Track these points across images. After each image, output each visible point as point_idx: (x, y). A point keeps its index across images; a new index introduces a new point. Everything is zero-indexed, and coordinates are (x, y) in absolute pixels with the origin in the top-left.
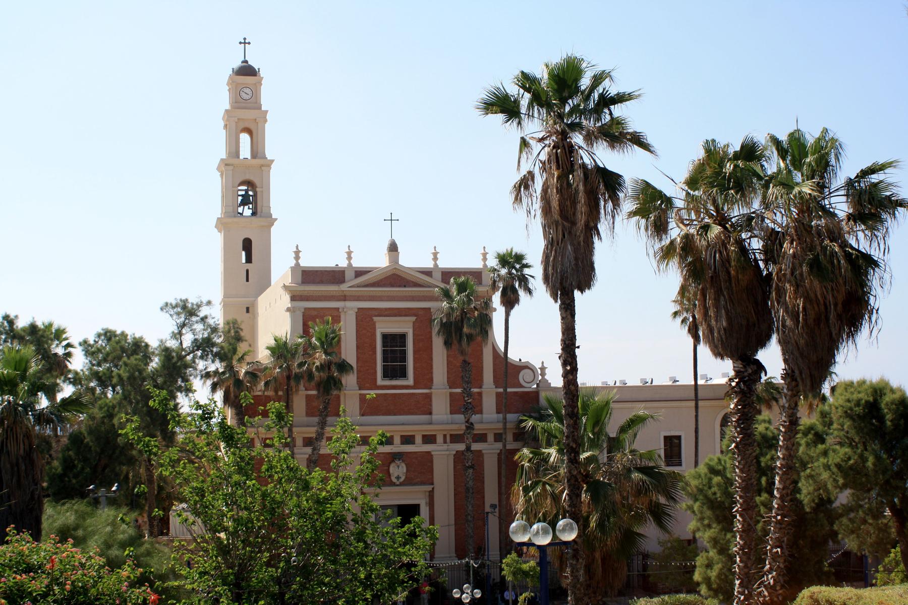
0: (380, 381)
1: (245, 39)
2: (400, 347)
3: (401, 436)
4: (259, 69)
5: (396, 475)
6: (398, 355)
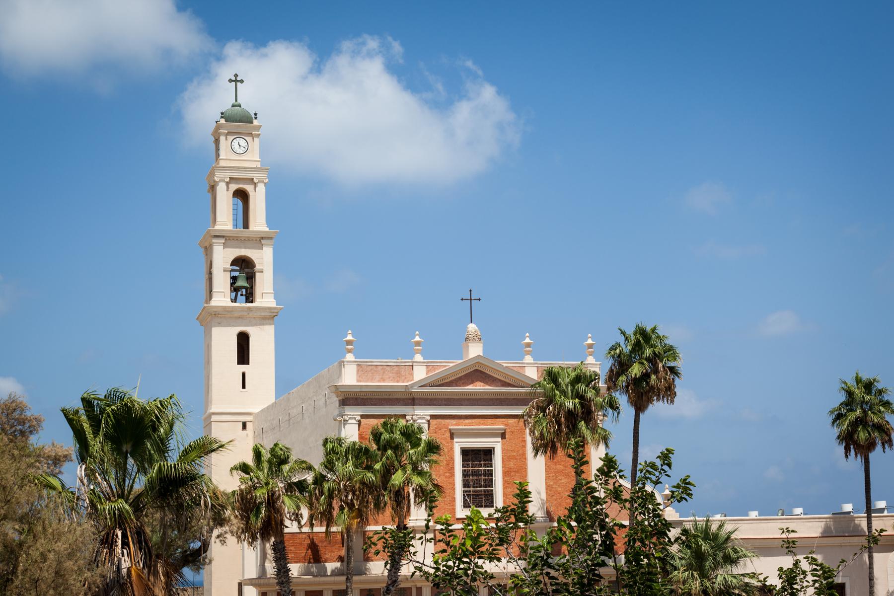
1: (236, 75)
2: (485, 465)
4: (256, 114)
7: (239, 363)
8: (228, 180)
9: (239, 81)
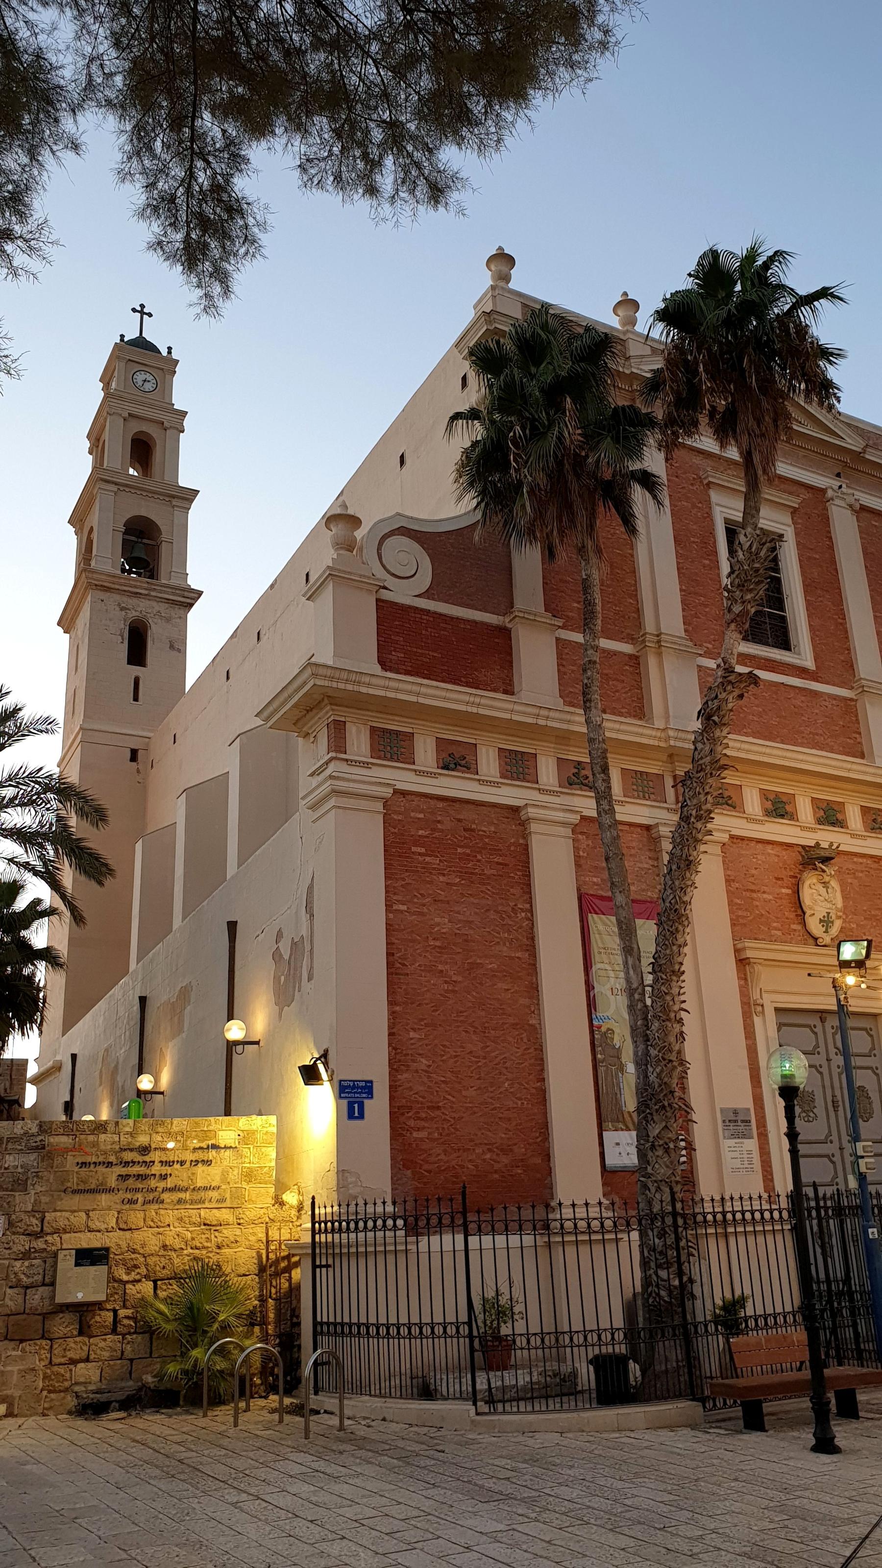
5: (821, 912)
7: (130, 662)
8: (126, 415)
9: (146, 314)
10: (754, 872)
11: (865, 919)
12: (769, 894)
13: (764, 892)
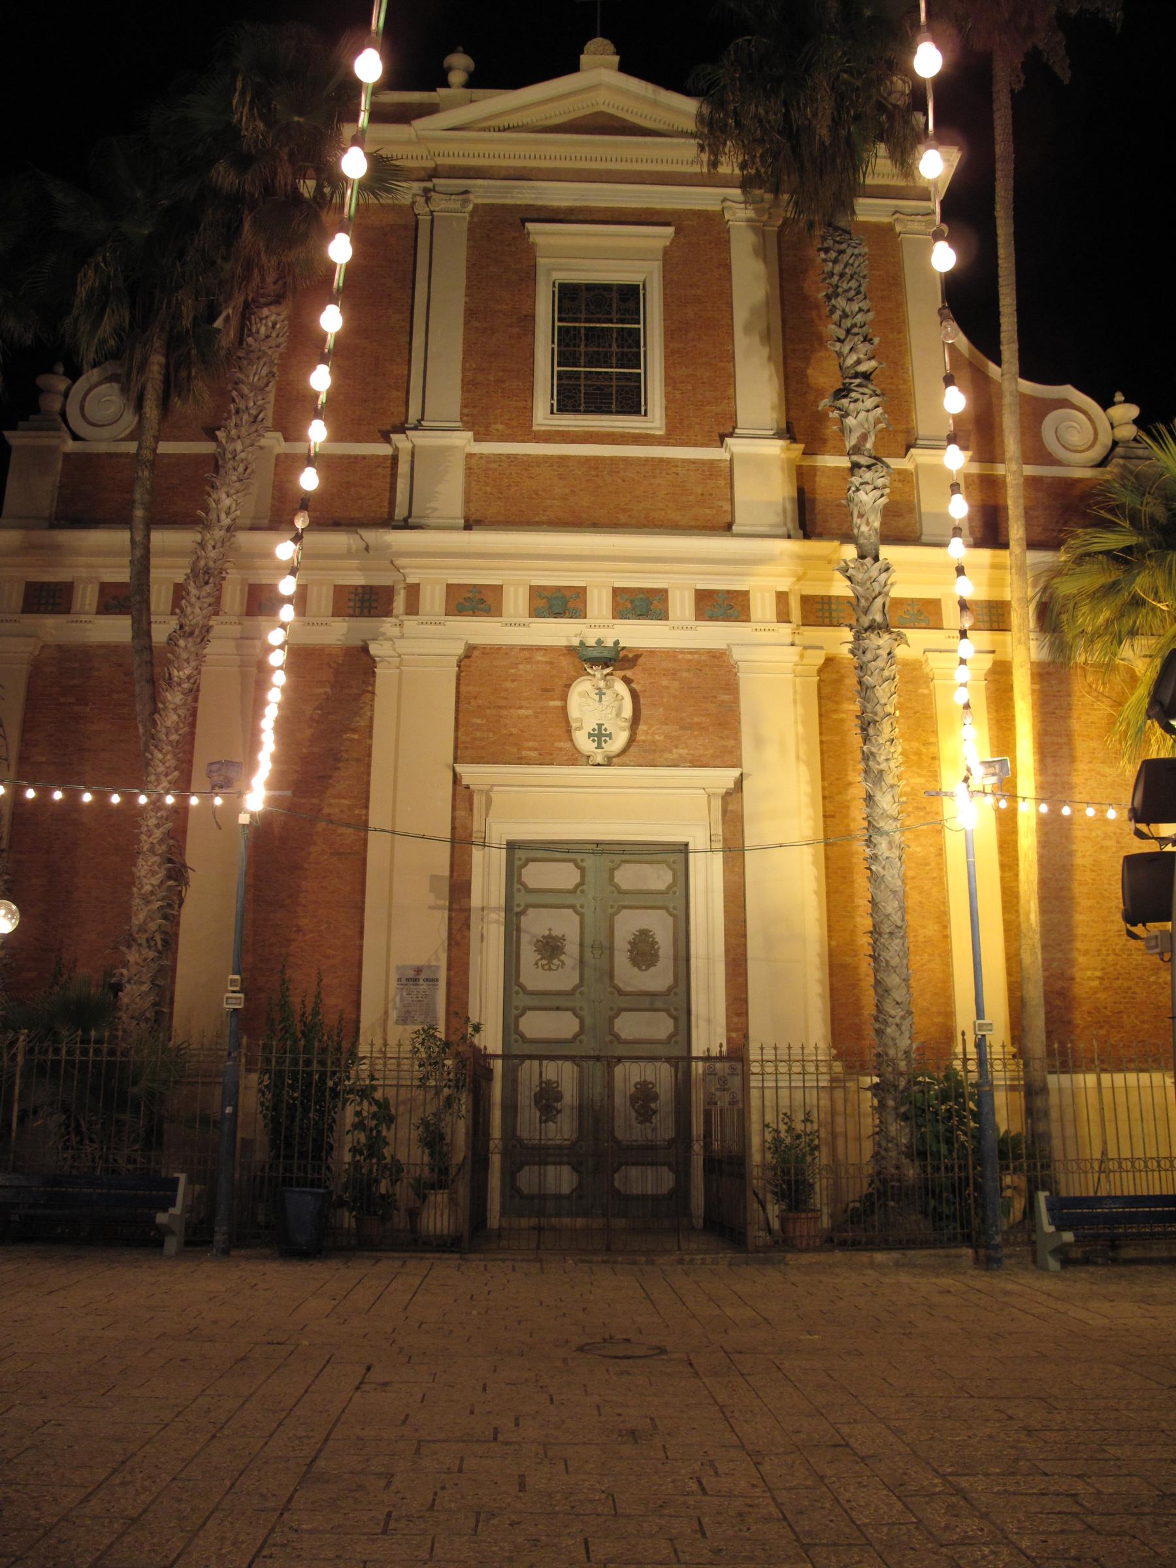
0: (543, 415)
3: (616, 591)
5: (590, 726)
6: (614, 348)
10: (508, 684)
11: (682, 728)
12: (527, 708)
13: (520, 708)
